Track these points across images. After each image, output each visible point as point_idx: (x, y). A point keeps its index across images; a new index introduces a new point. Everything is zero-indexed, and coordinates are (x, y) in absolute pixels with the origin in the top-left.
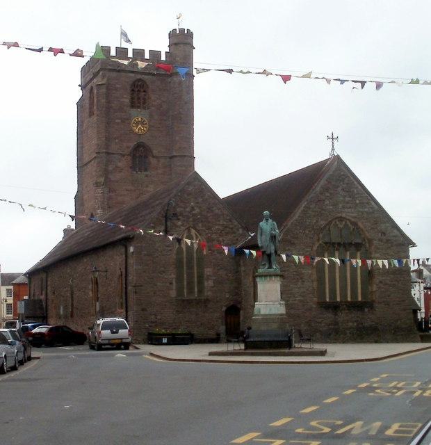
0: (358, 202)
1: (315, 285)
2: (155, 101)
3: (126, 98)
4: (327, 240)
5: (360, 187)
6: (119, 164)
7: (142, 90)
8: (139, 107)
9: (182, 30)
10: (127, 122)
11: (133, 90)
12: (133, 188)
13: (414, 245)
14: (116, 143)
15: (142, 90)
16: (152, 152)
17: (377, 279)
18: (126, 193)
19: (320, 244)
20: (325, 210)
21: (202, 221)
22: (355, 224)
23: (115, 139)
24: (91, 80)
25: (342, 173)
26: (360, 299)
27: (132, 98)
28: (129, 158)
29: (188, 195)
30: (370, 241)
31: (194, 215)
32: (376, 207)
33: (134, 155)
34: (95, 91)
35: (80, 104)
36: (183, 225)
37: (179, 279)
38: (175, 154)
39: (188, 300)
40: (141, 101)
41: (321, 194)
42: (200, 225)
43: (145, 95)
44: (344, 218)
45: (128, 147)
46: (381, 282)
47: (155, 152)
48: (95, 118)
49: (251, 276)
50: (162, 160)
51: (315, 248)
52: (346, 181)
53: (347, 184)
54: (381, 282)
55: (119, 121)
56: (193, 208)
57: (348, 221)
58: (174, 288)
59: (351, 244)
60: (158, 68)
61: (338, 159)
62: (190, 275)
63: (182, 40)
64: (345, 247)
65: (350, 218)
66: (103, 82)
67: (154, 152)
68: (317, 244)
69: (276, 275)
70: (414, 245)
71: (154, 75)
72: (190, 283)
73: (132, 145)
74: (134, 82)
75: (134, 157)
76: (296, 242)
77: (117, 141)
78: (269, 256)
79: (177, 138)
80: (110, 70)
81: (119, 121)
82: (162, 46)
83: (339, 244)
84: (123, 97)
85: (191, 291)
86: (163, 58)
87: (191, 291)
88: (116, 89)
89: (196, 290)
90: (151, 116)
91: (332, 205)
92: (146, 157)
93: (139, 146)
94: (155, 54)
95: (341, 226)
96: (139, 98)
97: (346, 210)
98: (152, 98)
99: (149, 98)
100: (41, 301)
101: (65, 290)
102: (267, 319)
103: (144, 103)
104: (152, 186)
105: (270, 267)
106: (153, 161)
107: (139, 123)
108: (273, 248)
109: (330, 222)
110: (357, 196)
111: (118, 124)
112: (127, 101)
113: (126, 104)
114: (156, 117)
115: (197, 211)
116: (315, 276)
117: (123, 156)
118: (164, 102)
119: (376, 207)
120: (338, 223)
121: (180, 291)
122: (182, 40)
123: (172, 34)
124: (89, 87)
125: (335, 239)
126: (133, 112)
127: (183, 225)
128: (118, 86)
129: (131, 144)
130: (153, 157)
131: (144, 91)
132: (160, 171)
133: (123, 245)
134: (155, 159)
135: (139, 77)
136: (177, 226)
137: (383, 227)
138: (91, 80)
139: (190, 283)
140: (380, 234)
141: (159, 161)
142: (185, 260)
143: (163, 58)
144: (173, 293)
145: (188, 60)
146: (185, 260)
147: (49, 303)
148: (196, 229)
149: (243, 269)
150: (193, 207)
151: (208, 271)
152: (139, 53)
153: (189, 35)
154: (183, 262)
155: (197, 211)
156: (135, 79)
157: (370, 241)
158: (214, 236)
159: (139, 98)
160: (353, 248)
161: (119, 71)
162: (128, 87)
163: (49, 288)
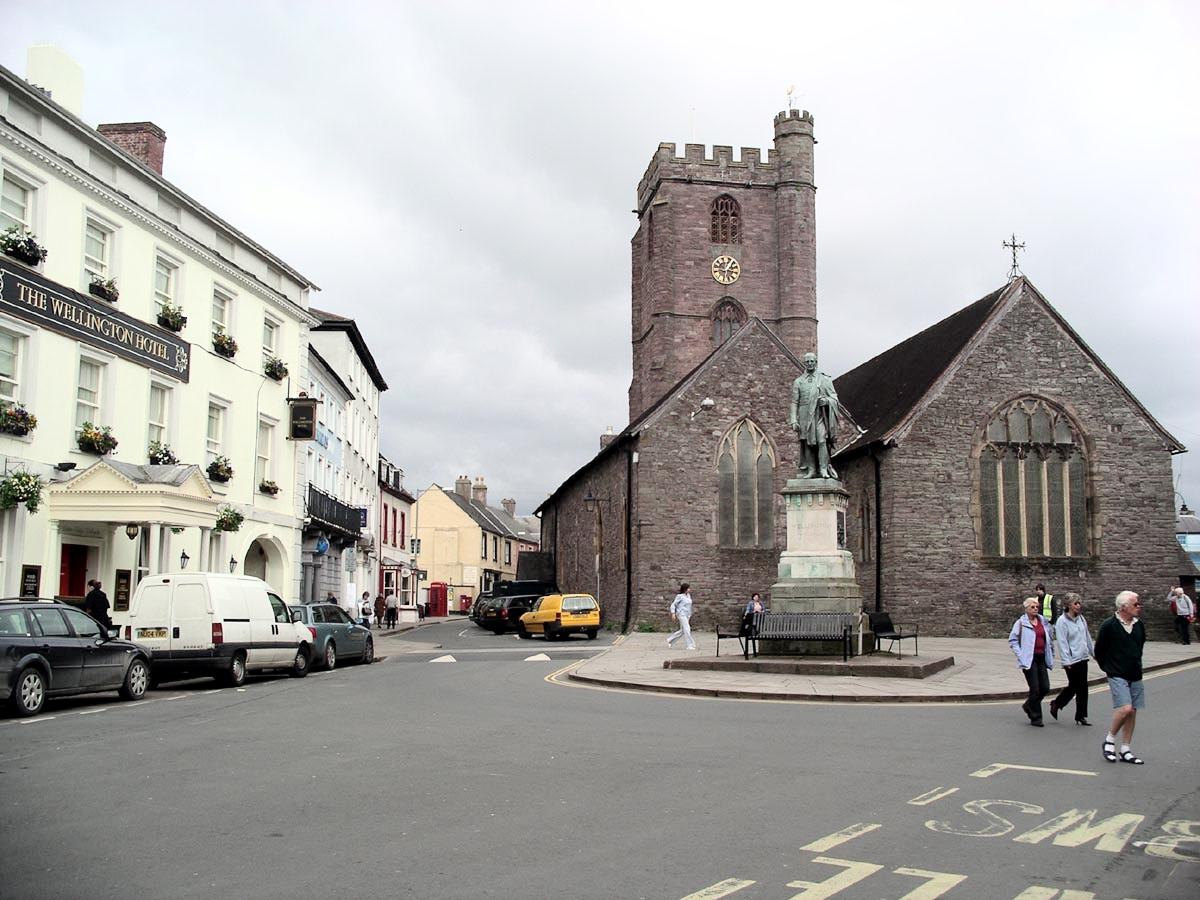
0: (1064, 366)
1: (978, 524)
2: (751, 229)
3: (703, 226)
4: (1002, 439)
5: (1067, 337)
6: (691, 333)
8: (724, 241)
9: (794, 113)
10: (703, 264)
11: (714, 213)
13: (1182, 450)
14: (686, 299)
17: (1103, 516)
19: (988, 446)
20: (997, 381)
21: (769, 407)
22: (1058, 407)
23: (685, 292)
24: (650, 199)
26: (1069, 554)
27: (714, 226)
29: (742, 359)
30: (1088, 440)
31: (752, 395)
35: (636, 242)
36: (731, 414)
37: (726, 513)
38: (784, 316)
39: (740, 552)
41: (990, 350)
42: (765, 413)
43: (735, 221)
45: (705, 306)
46: (1112, 521)
49: (859, 507)
51: (977, 453)
54: (1112, 521)
55: (688, 263)
57: (1044, 402)
58: (714, 527)
59: (1049, 446)
60: (754, 177)
62: (746, 507)
63: (793, 128)
64: (1038, 452)
65: (1047, 396)
67: (750, 312)
68: (981, 446)
69: (827, 493)
70: (1182, 450)
71: (748, 187)
72: (746, 521)
73: (713, 301)
74: (716, 201)
76: (938, 440)
78: (815, 449)
80: (676, 180)
81: (692, 263)
82: (764, 141)
83: (1026, 447)
84: (700, 226)
85: (747, 532)
86: (764, 159)
87: (747, 532)
88: (686, 211)
89: (757, 533)
90: (745, 254)
91: (1011, 372)
93: (726, 302)
94: (750, 153)
95: (1031, 412)
96: (724, 227)
97: (1041, 381)
100: (522, 556)
102: (813, 590)
103: (733, 234)
105: (818, 475)
107: (727, 267)
108: (822, 430)
109: (1008, 404)
110: (1060, 354)
111: (690, 267)
112: (704, 230)
113: (701, 235)
114: (754, 256)
115: (759, 388)
116: (976, 509)
118: (765, 230)
120: (1023, 404)
121: (726, 536)
122: (793, 128)
123: (779, 121)
125: (1019, 437)
127: (731, 414)
129: (710, 300)
131: (733, 215)
133: (625, 451)
135: (724, 191)
136: (721, 416)
137: (1116, 414)
138: (650, 199)
139: (746, 521)
140: (1110, 427)
142: (736, 478)
143: (764, 159)
144: (713, 539)
146: (736, 478)
147: (558, 558)
148: (756, 421)
150: (751, 381)
154: (732, 482)
155: (759, 388)
156: (716, 195)
160: (1053, 455)
161: (690, 182)
163: (558, 532)
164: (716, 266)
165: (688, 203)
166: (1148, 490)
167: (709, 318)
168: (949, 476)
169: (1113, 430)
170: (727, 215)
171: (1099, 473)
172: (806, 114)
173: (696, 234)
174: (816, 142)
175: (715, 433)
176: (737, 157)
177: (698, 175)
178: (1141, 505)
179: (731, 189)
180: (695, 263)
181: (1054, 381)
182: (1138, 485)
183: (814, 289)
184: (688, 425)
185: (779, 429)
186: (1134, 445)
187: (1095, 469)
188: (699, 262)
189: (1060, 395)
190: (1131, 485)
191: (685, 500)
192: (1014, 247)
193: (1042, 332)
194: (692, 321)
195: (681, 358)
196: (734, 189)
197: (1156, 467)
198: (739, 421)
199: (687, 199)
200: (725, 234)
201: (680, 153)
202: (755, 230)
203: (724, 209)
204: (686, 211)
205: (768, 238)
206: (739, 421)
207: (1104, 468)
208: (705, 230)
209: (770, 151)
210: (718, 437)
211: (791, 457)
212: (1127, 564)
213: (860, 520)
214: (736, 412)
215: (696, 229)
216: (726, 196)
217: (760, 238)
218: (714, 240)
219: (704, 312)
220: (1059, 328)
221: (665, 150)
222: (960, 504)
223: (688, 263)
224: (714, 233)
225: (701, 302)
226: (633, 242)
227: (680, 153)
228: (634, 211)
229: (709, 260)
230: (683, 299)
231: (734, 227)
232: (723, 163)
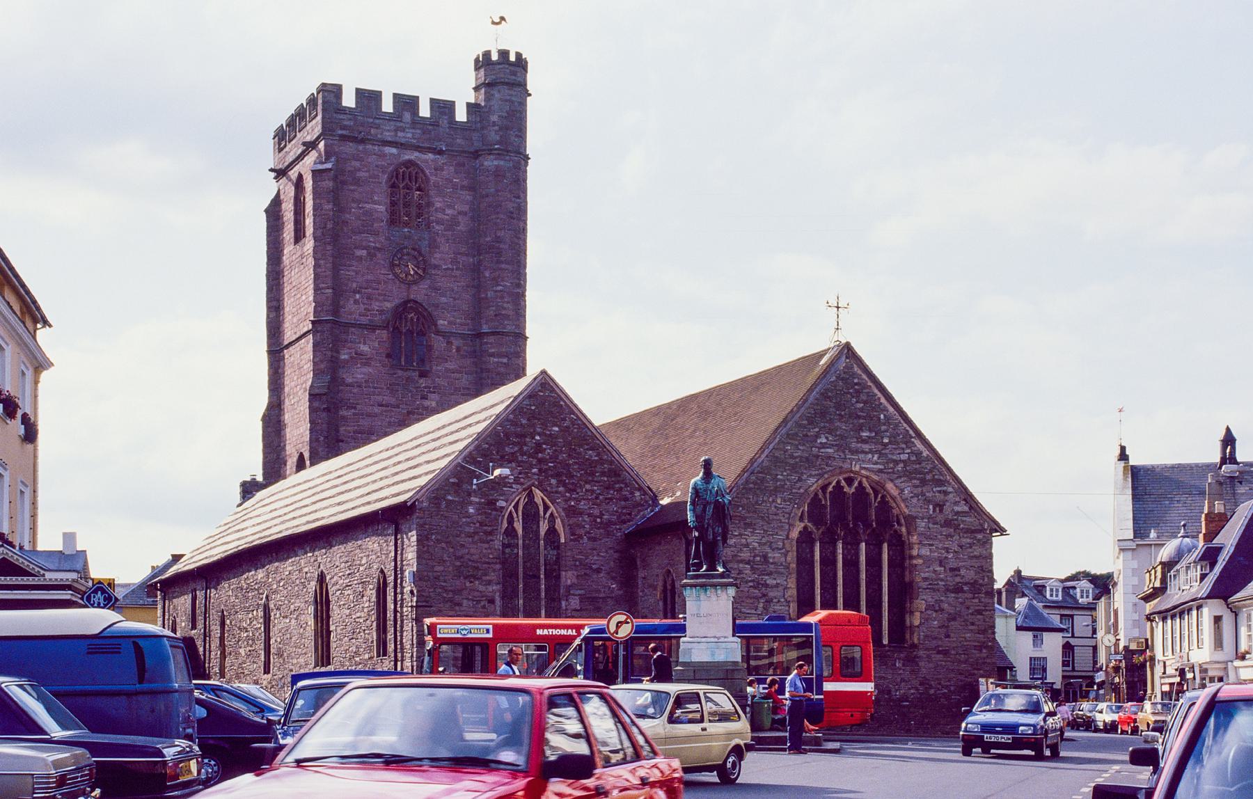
0: (886, 440)
5: (891, 409)
8: (406, 224)
9: (504, 54)
11: (393, 186)
12: (393, 401)
13: (1002, 531)
14: (356, 302)
16: (436, 325)
18: (377, 410)
23: (355, 292)
25: (856, 381)
27: (393, 204)
28: (384, 334)
31: (540, 461)
32: (926, 453)
34: (309, 184)
35: (274, 212)
38: (485, 329)
40: (414, 210)
42: (553, 481)
43: (421, 197)
44: (856, 473)
45: (381, 312)
48: (309, 244)
49: (660, 588)
51: (795, 534)
52: (864, 397)
53: (865, 402)
55: (359, 253)
56: (538, 447)
57: (864, 479)
58: (498, 609)
61: (847, 351)
66: (329, 166)
67: (441, 322)
70: (1002, 531)
75: (396, 332)
79: (490, 294)
81: (364, 253)
86: (461, 115)
88: (357, 182)
92: (422, 334)
94: (443, 108)
96: (407, 205)
98: (438, 205)
99: (429, 204)
101: (588, 487)
106: (438, 343)
111: (360, 258)
113: (376, 215)
118: (459, 213)
119: (926, 453)
123: (483, 63)
124: (293, 174)
128: (359, 174)
130: (438, 333)
131: (419, 189)
140: (931, 507)
141: (449, 343)
143: (461, 115)
145: (515, 121)
149: (641, 574)
150: (538, 444)
151: (568, 577)
152: (406, 103)
153: (521, 64)
157: (910, 521)
158: (583, 505)
159: (407, 205)
166: (969, 575)
167: (386, 327)
168: (765, 557)
169: (934, 511)
171: (919, 556)
172: (519, 55)
173: (368, 213)
174: (530, 95)
175: (501, 503)
176: (425, 111)
178: (958, 590)
180: (369, 254)
181: (876, 458)
182: (958, 569)
183: (522, 296)
184: (469, 495)
185: (570, 499)
186: (957, 527)
187: (915, 552)
189: (880, 471)
190: (952, 570)
191: (465, 578)
192: (838, 307)
193: (865, 402)
195: (349, 380)
197: (977, 551)
198: (524, 490)
201: (349, 100)
202: (449, 211)
203: (407, 180)
205: (463, 225)
206: (524, 490)
207: (925, 551)
208: (382, 208)
209: (469, 105)
210: (503, 508)
211: (582, 532)
212: (945, 653)
213: (661, 603)
214: (522, 480)
215: (368, 206)
216: (409, 164)
217: (453, 222)
220: (883, 400)
221: (331, 92)
222: (777, 585)
223: (359, 253)
224: (392, 213)
225: (375, 306)
226: (266, 211)
227: (349, 100)
228: (271, 170)
231: (419, 206)
232: (407, 116)
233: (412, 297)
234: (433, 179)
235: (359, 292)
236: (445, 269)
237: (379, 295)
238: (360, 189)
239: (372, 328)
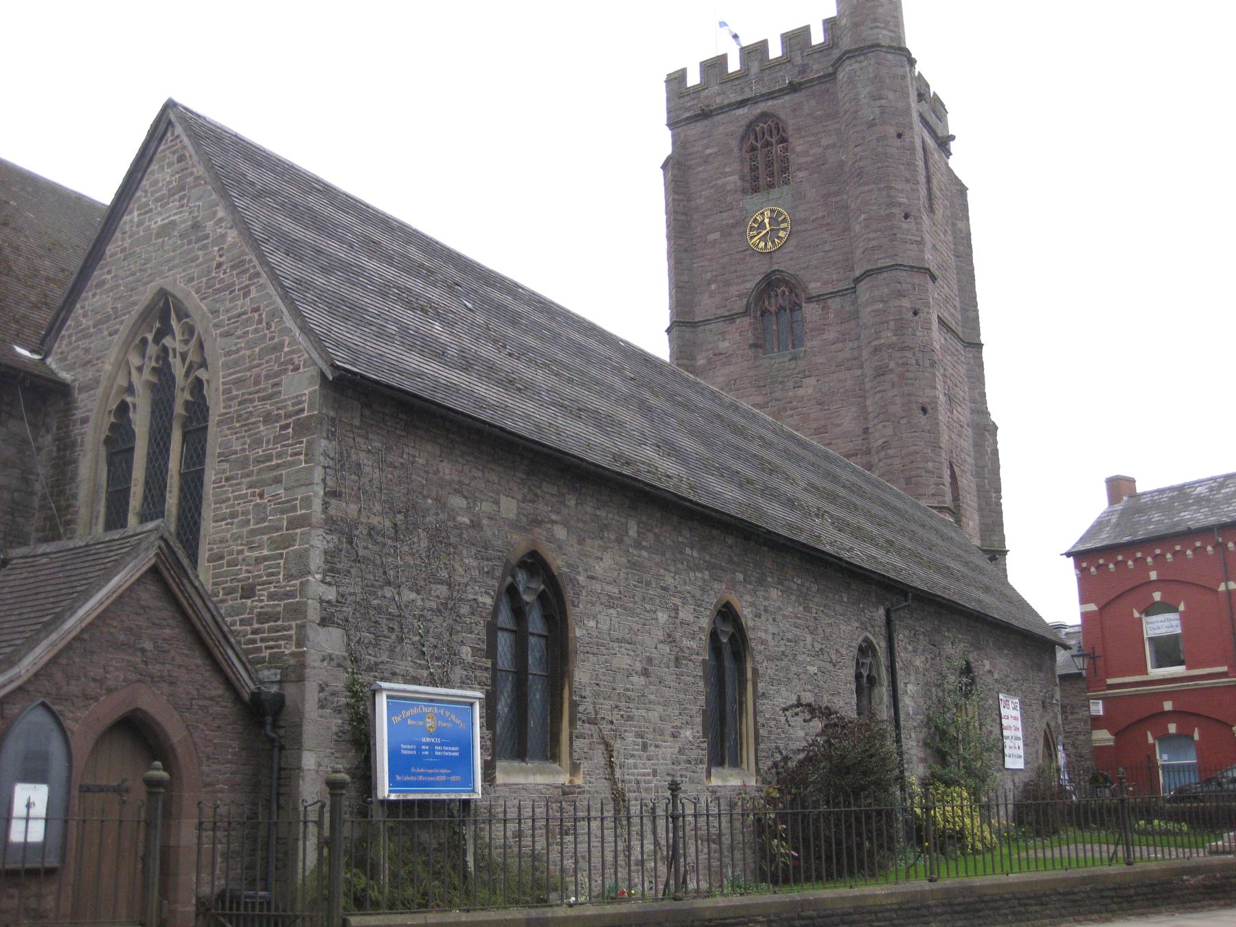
3: (732, 174)
6: (724, 345)
7: (774, 141)
8: (771, 186)
10: (735, 231)
11: (753, 149)
15: (774, 141)
33: (764, 313)
47: (814, 287)
50: (835, 303)
55: (711, 237)
60: (804, 69)
67: (812, 285)
77: (713, 287)
81: (716, 235)
84: (726, 175)
92: (796, 306)
93: (771, 283)
96: (769, 164)
98: (798, 149)
104: (813, 381)
113: (728, 188)
117: (731, 318)
118: (827, 147)
126: (751, 201)
130: (810, 299)
132: (831, 335)
134: (814, 305)
156: (744, 122)
162: (734, 144)
164: (752, 228)
165: (707, 147)
167: (745, 313)
170: (768, 144)
177: (718, 100)
179: (770, 103)
188: (726, 232)
194: (721, 326)
196: (775, 102)
199: (705, 141)
200: (771, 175)
204: (706, 161)
215: (719, 182)
216: (764, 116)
218: (756, 190)
219: (739, 306)
221: (676, 80)
223: (711, 237)
225: (734, 290)
229: (742, 222)
230: (706, 296)
233: (776, 267)
234: (791, 122)
235: (715, 281)
236: (813, 221)
237: (738, 277)
238: (709, 167)
239: (731, 318)
